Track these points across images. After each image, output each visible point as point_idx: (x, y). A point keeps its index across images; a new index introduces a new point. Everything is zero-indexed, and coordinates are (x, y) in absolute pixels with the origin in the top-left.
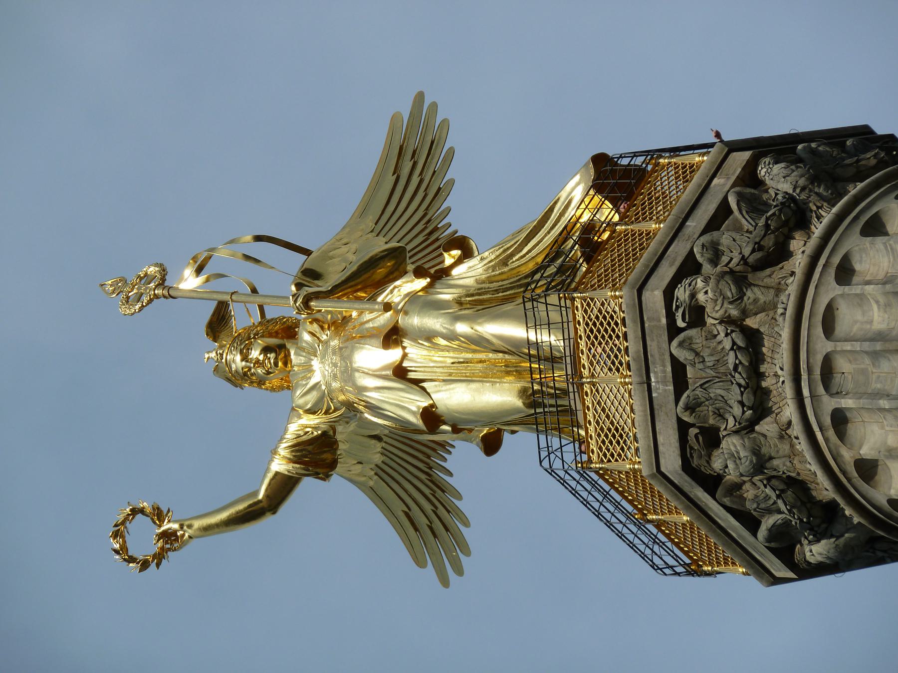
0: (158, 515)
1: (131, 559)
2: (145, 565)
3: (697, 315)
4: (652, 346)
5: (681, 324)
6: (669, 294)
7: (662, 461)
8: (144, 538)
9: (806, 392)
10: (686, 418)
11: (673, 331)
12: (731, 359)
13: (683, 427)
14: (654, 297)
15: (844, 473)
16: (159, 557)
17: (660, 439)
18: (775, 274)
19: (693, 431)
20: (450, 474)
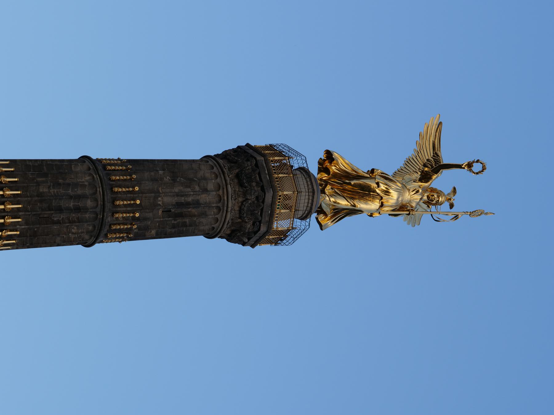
0: (471, 170)
1: (481, 163)
2: (478, 161)
3: (254, 224)
4: (267, 219)
5: (258, 223)
6: (259, 230)
7: (272, 195)
8: (477, 167)
9: (225, 208)
10: (262, 204)
11: (260, 222)
12: (245, 215)
13: (263, 202)
14: (263, 229)
15: (223, 188)
16: (474, 162)
17: (271, 200)
18: (233, 228)
19: (261, 201)
20: (415, 150)
